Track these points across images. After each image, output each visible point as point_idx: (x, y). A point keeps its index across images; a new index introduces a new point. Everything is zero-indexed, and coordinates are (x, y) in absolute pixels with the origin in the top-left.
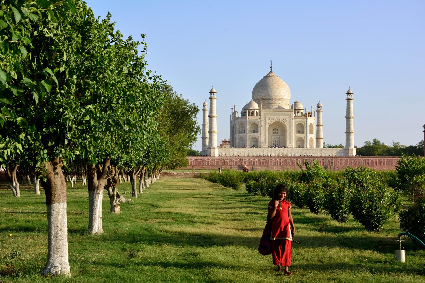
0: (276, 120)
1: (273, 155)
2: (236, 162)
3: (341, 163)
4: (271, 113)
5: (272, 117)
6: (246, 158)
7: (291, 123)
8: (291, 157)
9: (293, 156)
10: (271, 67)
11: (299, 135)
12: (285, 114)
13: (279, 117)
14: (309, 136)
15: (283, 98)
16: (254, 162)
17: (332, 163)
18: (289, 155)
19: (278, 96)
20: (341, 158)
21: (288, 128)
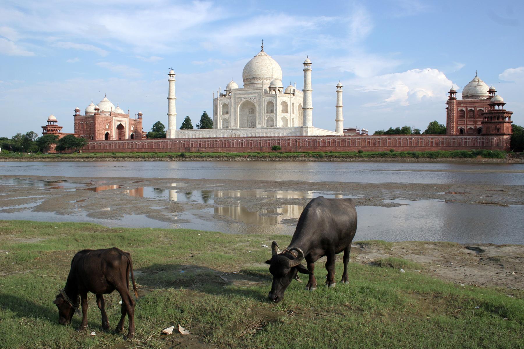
0: (245, 100)
1: (226, 136)
2: (184, 144)
3: (289, 144)
4: (241, 92)
5: (241, 96)
6: (193, 140)
7: (260, 101)
8: (244, 137)
9: (245, 136)
10: (262, 47)
11: (269, 115)
12: (254, 93)
13: (248, 96)
14: (280, 114)
15: (265, 76)
16: (200, 144)
17: (279, 143)
18: (242, 136)
19: (258, 75)
20: (289, 138)
21: (257, 107)
